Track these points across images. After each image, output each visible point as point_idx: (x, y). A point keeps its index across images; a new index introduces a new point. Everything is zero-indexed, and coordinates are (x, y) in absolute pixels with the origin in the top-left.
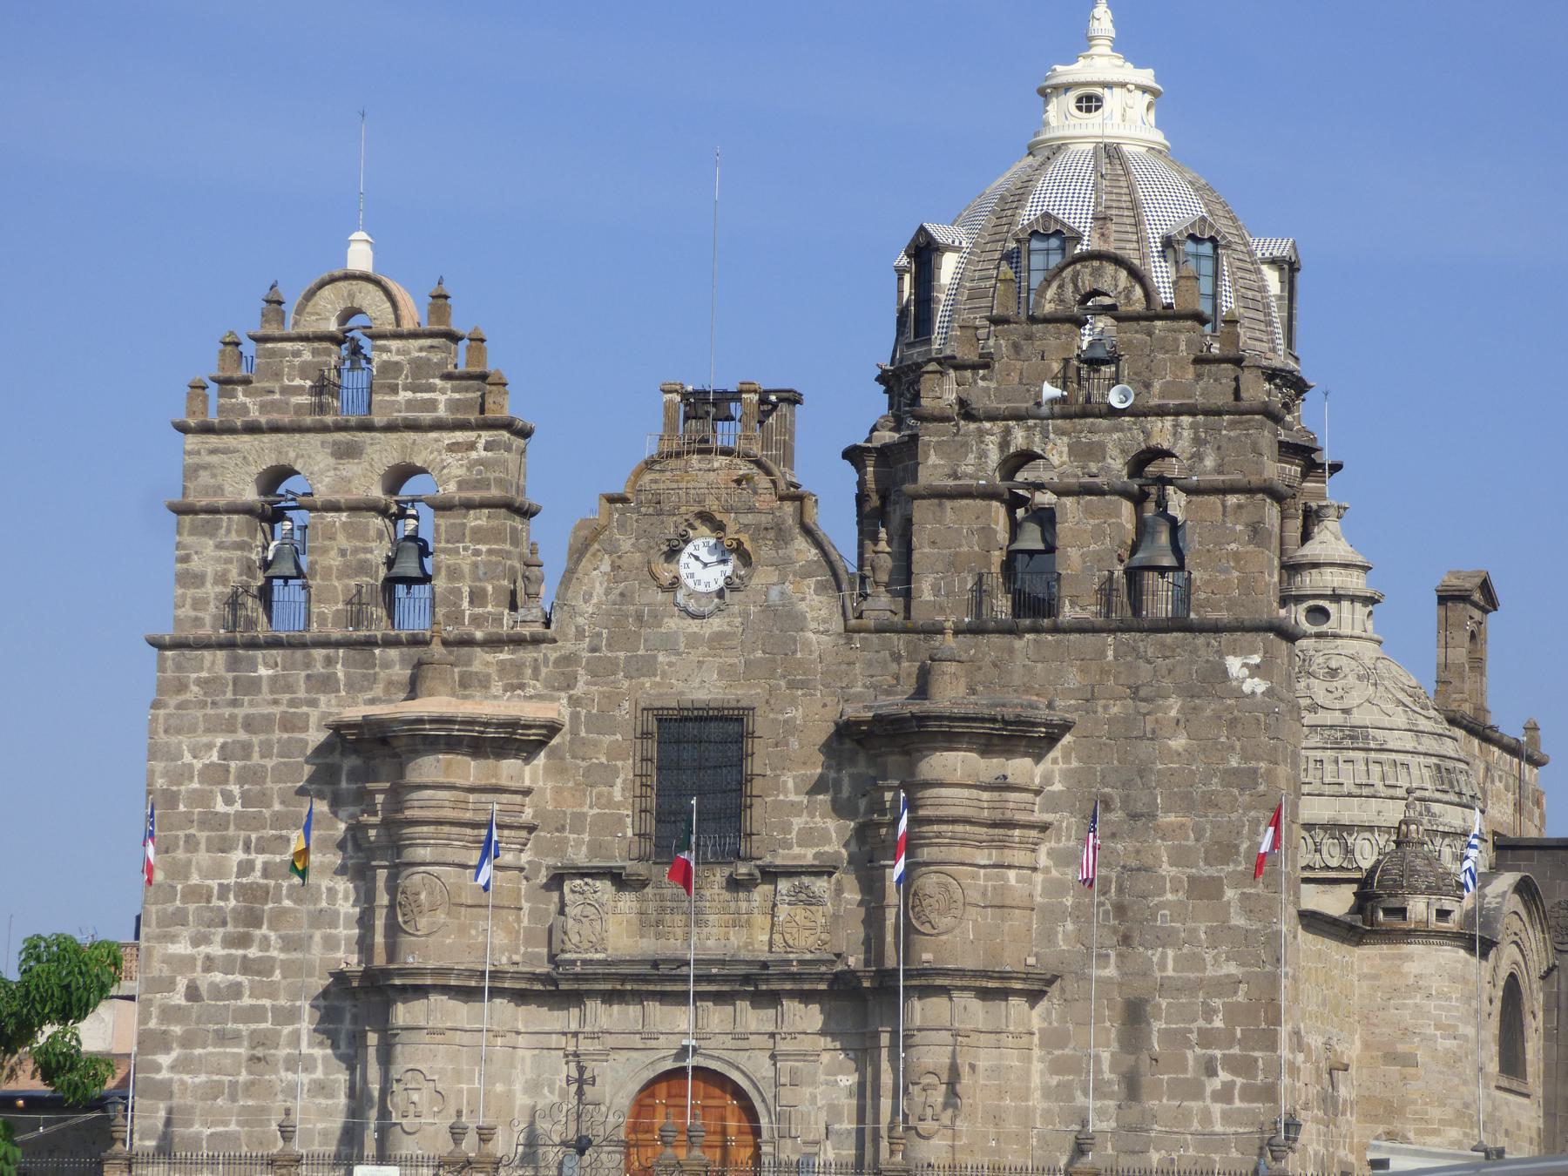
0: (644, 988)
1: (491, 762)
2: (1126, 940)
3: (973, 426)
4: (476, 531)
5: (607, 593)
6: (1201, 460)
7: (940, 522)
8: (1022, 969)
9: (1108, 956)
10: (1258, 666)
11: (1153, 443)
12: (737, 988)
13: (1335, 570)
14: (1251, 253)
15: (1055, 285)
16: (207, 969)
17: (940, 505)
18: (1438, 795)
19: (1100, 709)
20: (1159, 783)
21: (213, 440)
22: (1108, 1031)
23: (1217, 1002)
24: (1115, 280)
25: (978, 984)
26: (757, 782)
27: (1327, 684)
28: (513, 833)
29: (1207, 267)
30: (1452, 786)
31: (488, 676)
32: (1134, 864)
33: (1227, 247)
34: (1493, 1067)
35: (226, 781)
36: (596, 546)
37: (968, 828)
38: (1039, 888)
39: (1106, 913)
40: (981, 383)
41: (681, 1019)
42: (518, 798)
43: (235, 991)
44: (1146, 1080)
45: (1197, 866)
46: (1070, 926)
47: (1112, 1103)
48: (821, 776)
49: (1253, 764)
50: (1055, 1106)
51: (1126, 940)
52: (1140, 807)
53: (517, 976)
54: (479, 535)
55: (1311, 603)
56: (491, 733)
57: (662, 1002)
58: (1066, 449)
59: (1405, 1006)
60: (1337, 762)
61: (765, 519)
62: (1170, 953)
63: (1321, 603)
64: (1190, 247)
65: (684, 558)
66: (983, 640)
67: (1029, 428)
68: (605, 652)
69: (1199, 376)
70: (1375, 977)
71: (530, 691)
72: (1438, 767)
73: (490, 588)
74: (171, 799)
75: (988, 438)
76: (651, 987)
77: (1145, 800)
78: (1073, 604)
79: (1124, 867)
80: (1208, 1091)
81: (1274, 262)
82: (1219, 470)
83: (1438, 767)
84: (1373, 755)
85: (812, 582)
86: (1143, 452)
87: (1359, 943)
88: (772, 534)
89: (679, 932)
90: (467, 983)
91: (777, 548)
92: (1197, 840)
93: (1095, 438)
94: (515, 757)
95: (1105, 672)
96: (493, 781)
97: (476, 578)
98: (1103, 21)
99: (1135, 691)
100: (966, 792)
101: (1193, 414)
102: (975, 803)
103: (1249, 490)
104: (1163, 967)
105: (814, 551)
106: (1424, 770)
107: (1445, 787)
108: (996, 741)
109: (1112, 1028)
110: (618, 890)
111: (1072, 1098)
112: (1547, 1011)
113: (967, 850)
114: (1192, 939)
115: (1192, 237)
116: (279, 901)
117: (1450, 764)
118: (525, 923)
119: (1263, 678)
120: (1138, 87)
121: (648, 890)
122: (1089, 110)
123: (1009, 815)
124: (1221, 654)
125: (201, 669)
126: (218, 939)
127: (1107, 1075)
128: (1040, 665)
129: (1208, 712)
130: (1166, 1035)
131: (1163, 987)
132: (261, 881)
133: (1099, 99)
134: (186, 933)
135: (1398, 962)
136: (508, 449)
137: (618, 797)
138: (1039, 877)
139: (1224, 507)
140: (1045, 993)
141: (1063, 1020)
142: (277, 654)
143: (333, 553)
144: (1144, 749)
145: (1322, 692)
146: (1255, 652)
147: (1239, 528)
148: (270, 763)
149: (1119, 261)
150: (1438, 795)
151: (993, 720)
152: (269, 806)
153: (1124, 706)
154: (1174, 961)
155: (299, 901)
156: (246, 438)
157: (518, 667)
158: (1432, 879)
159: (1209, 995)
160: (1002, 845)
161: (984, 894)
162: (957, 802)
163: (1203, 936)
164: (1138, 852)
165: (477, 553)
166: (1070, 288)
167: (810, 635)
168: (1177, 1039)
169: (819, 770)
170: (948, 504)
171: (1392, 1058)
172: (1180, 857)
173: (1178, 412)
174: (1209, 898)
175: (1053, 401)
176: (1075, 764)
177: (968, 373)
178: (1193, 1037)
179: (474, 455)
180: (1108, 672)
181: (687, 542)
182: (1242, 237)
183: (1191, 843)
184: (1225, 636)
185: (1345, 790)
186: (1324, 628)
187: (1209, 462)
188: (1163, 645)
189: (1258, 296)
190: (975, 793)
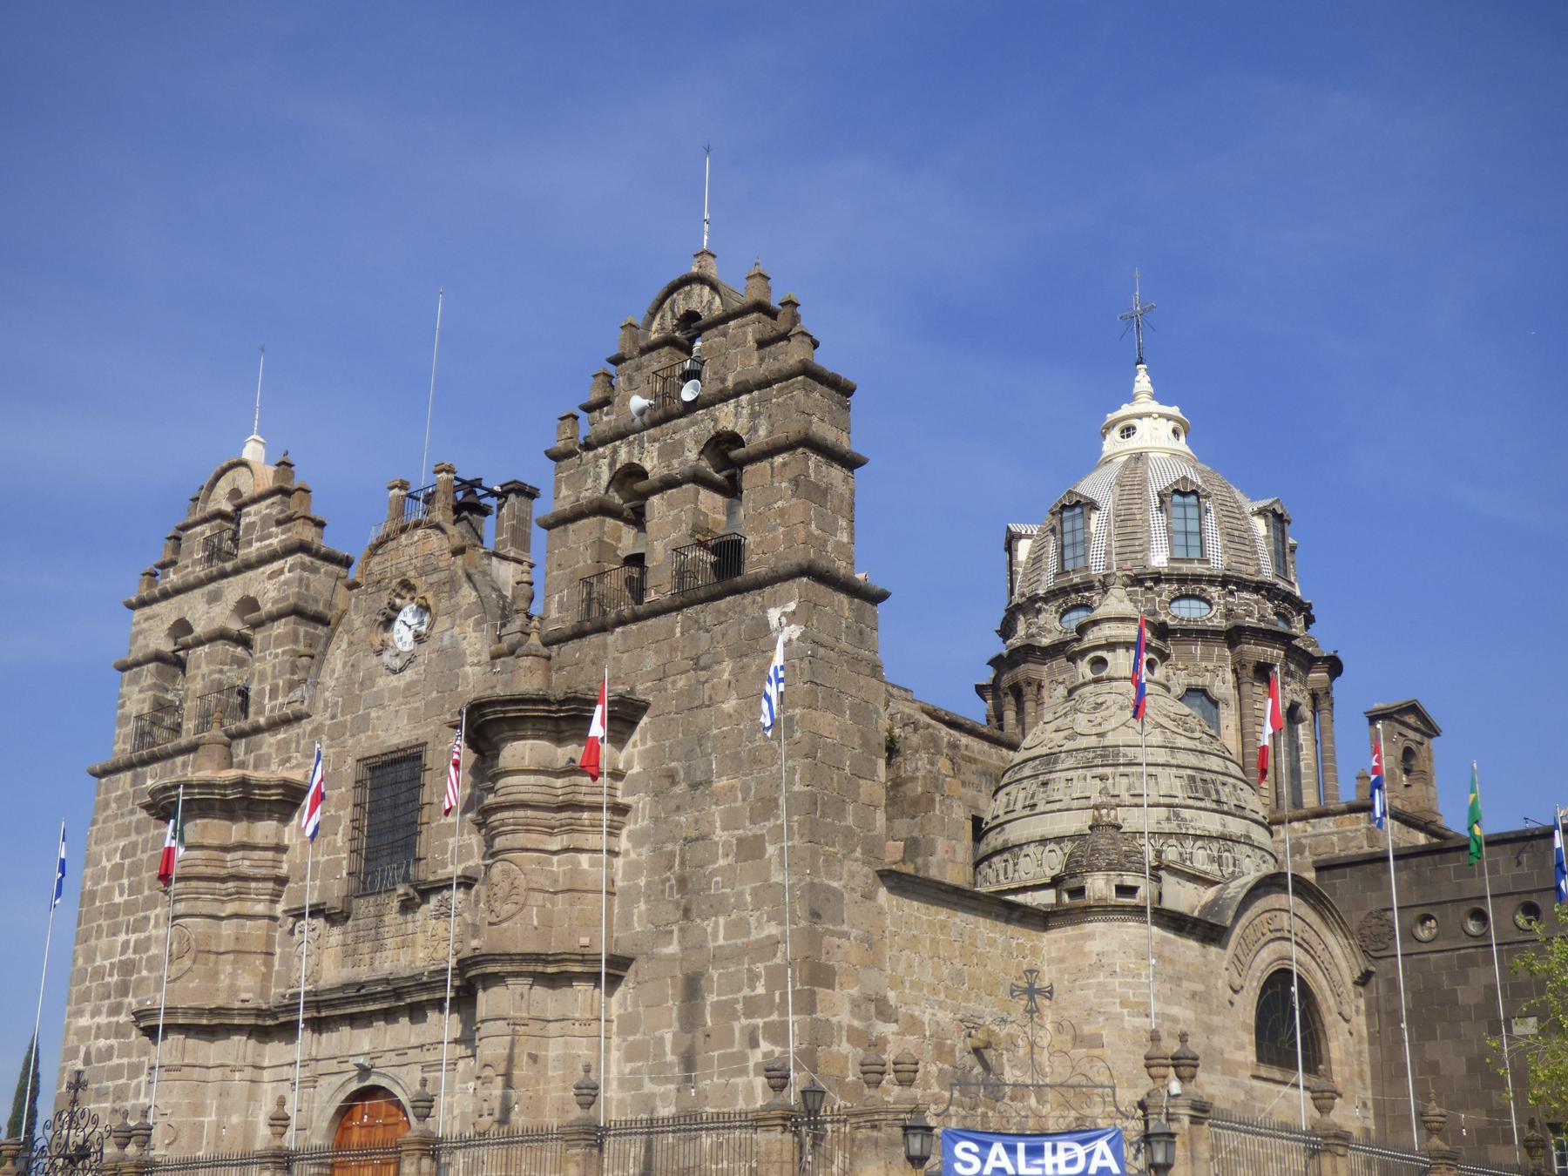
0: (338, 1012)
1: (244, 824)
2: (686, 913)
3: (591, 454)
4: (277, 638)
5: (344, 666)
6: (756, 431)
10: (794, 613)
11: (720, 427)
13: (1112, 625)
14: (1240, 508)
15: (658, 317)
16: (97, 1037)
20: (714, 748)
21: (147, 610)
22: (670, 1009)
23: (760, 967)
24: (700, 299)
25: (531, 969)
26: (426, 810)
27: (1091, 717)
28: (260, 885)
29: (1192, 512)
30: (1207, 793)
32: (694, 834)
33: (1207, 497)
34: (1249, 1054)
35: (121, 877)
37: (530, 813)
39: (671, 887)
40: (605, 418)
41: (361, 1042)
42: (270, 855)
43: (108, 1053)
44: (699, 1058)
45: (744, 828)
46: (643, 906)
47: (672, 1087)
48: (470, 795)
50: (628, 1095)
51: (686, 913)
53: (243, 1012)
54: (279, 641)
55: (1092, 655)
56: (232, 795)
57: (352, 1025)
58: (655, 454)
59: (1089, 986)
61: (443, 575)
62: (722, 920)
63: (1099, 653)
64: (1177, 499)
65: (398, 625)
66: (586, 641)
67: (630, 444)
68: (340, 718)
69: (762, 359)
70: (1061, 960)
71: (294, 762)
72: (1192, 779)
74: (93, 895)
75: (602, 461)
80: (751, 1064)
81: (1261, 513)
82: (770, 433)
83: (1192, 779)
84: (1122, 769)
85: (471, 621)
87: (1046, 928)
88: (447, 588)
89: (367, 957)
90: (196, 1021)
93: (676, 437)
94: (270, 818)
95: (673, 649)
97: (275, 677)
98: (1143, 382)
99: (696, 659)
100: (532, 779)
101: (750, 391)
102: (543, 789)
103: (789, 447)
104: (715, 937)
106: (1178, 782)
107: (1200, 795)
108: (564, 726)
109: (673, 1006)
111: (640, 1085)
112: (1369, 1015)
113: (534, 836)
114: (740, 905)
115: (1177, 492)
117: (1207, 776)
118: (276, 967)
119: (798, 624)
120: (1161, 416)
121: (350, 923)
123: (580, 797)
124: (764, 609)
127: (670, 1058)
130: (717, 1006)
131: (721, 957)
134: (89, 1007)
136: (314, 570)
137: (339, 843)
138: (619, 862)
141: (635, 1004)
142: (157, 766)
143: (199, 679)
144: (702, 716)
148: (145, 856)
149: (701, 280)
151: (545, 701)
152: (141, 892)
153: (689, 679)
155: (150, 970)
156: (164, 603)
157: (287, 742)
159: (753, 961)
161: (556, 881)
162: (522, 789)
163: (749, 898)
164: (697, 821)
165: (276, 656)
166: (669, 315)
167: (468, 669)
168: (726, 1011)
170: (571, 527)
171: (1078, 1040)
172: (731, 822)
173: (737, 394)
174: (754, 858)
175: (642, 412)
176: (649, 744)
177: (597, 413)
178: (739, 1007)
179: (282, 578)
180: (676, 649)
181: (398, 610)
183: (739, 804)
184: (768, 590)
186: (1104, 674)
187: (762, 432)
188: (719, 611)
190: (543, 779)
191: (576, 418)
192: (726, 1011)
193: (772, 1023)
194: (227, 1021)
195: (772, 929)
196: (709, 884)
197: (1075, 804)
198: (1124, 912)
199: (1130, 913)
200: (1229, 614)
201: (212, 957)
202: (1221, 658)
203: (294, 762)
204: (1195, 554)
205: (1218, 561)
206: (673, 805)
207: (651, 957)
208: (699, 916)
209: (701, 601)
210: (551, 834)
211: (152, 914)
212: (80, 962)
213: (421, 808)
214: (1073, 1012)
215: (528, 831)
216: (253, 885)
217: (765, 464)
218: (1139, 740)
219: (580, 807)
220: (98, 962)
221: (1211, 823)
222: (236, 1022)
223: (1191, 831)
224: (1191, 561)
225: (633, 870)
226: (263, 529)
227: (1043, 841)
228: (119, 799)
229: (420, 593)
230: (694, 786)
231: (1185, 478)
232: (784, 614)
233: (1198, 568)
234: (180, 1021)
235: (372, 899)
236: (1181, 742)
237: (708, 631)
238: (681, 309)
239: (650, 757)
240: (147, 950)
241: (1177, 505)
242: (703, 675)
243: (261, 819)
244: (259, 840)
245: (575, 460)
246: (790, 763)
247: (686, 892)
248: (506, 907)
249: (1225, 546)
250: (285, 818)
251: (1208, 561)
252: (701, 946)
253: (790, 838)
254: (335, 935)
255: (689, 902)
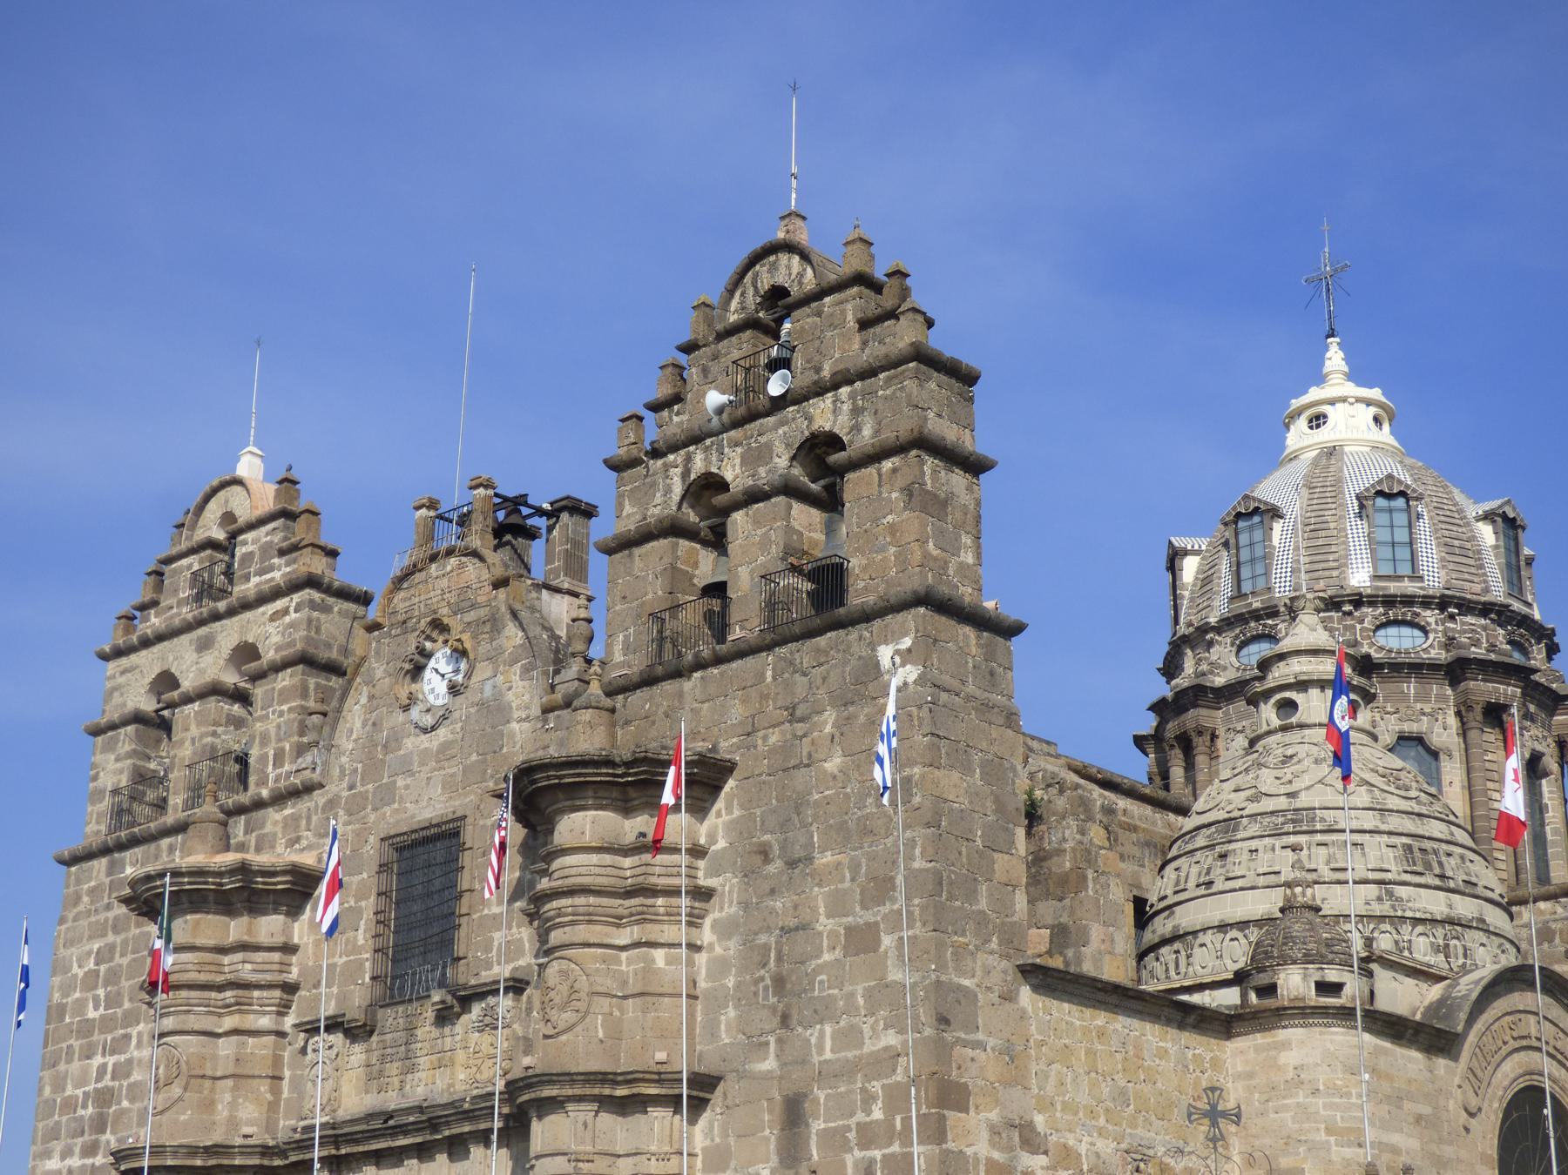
1: (245, 919)
2: (785, 1020)
3: (660, 462)
4: (281, 692)
5: (364, 725)
6: (860, 430)
7: (629, 574)
8: (655, 1068)
9: (767, 1044)
10: (909, 650)
11: (815, 427)
12: (429, 1138)
13: (1303, 659)
14: (1460, 511)
17: (630, 555)
18: (1407, 878)
19: (760, 742)
20: (816, 817)
21: (124, 662)
22: (767, 1139)
23: (876, 1086)
24: (788, 272)
25: (596, 1091)
27: (1279, 773)
28: (265, 994)
29: (1401, 519)
31: (275, 834)
33: (1417, 499)
35: (95, 987)
36: (358, 680)
37: (592, 900)
38: (703, 971)
39: (766, 989)
40: (676, 419)
42: (276, 956)
45: (854, 914)
48: (520, 880)
49: (907, 771)
51: (785, 1020)
52: (798, 852)
54: (284, 696)
55: (1278, 696)
56: (229, 884)
57: (378, 1165)
58: (738, 461)
59: (1286, 1108)
60: (1273, 849)
61: (483, 612)
62: (828, 1029)
63: (1287, 694)
64: (1381, 502)
65: (428, 674)
66: (656, 690)
67: (707, 449)
68: (360, 789)
69: (865, 343)
70: (1250, 1075)
71: (304, 843)
72: (1408, 848)
73: (288, 747)
74: (61, 1010)
75: (673, 471)
76: (361, 1149)
77: (802, 840)
78: (742, 628)
79: (782, 929)
81: (1488, 517)
82: (877, 432)
83: (1408, 848)
84: (1319, 837)
85: (517, 668)
86: (807, 440)
87: (1228, 1034)
88: (487, 628)
89: (396, 1081)
90: (189, 1162)
91: (492, 640)
92: (853, 880)
93: (763, 440)
94: (276, 911)
95: (764, 697)
96: (246, 938)
97: (280, 740)
98: (1335, 359)
99: (792, 709)
100: (594, 858)
101: (850, 382)
102: (609, 871)
103: (900, 449)
104: (821, 1050)
105: (521, 634)
106: (1391, 853)
107: (1419, 869)
108: (632, 793)
109: (770, 1135)
110: (353, 1042)
113: (598, 928)
114: (851, 1009)
115: (1380, 493)
116: (119, 1103)
117: (1427, 845)
118: (285, 1095)
119: (914, 663)
120: (1358, 400)
121: (374, 1038)
122: (1318, 426)
123: (654, 880)
125: (90, 879)
126: (77, 1150)
128: (706, 705)
129: (862, 719)
130: (824, 1134)
131: (828, 1074)
132: (110, 1084)
133: (1325, 416)
134: (58, 1146)
135: (1273, 1053)
136: (326, 609)
137: (361, 942)
138: (702, 959)
139: (880, 475)
140: (708, 1101)
142: (138, 851)
143: (187, 743)
145: (1270, 780)
146: (906, 635)
147: (894, 495)
148: (125, 961)
149: (789, 247)
150: (1407, 878)
151: (609, 763)
153: (783, 733)
154: (833, 1038)
155: (132, 1100)
156: (144, 653)
157: (295, 818)
158: (1311, 946)
159: (868, 1078)
160: (642, 918)
161: (625, 982)
162: (583, 870)
163: (861, 1001)
164: (796, 907)
165: (281, 714)
166: (751, 292)
167: (514, 726)
168: (836, 1141)
169: (517, 874)
170: (637, 551)
172: (837, 907)
173: (835, 386)
174: (866, 951)
175: (720, 411)
176: (737, 813)
177: (665, 413)
178: (852, 1135)
179: (287, 619)
181: (429, 656)
182: (1452, 499)
183: (847, 885)
184: (877, 623)
185: (1283, 879)
186: (1294, 720)
187: (867, 432)
188: (818, 650)
189: (1468, 545)
190: (607, 859)
191: (641, 419)
192: (836, 1141)
193: (893, 1155)
194: (226, 1162)
195: (891, 1039)
196: (812, 983)
197: (1262, 881)
198: (1327, 1015)
199: (1334, 1016)
200: (1449, 643)
201: (208, 1083)
202: (1442, 698)
203: (304, 843)
204: (1405, 569)
205: (1434, 578)
206: (766, 887)
207: (742, 1075)
208: (800, 1023)
209: (796, 639)
210: (618, 926)
211: (134, 1032)
212: (47, 1091)
213: (460, 896)
214: (1267, 1141)
215: (590, 922)
216: (256, 993)
217: (871, 471)
218: (1340, 801)
219: (653, 892)
220: (69, 1091)
221: (1435, 903)
222: (237, 1162)
223: (1409, 914)
224: (1399, 578)
225: (719, 967)
226: (262, 562)
227: (1223, 927)
228: (92, 892)
229: (455, 634)
230: (792, 864)
231: (1390, 477)
232: (897, 652)
233: (1409, 587)
234: (169, 1163)
235: (401, 1009)
236: (1394, 802)
237: (805, 675)
238: (765, 284)
239: (739, 830)
240: (128, 1075)
241: (1381, 510)
242: (800, 728)
243: (265, 913)
244: (263, 938)
245: (640, 470)
246: (908, 834)
247: (784, 995)
248: (564, 1016)
249: (1442, 560)
250: (294, 912)
251: (1421, 578)
252: (804, 1062)
253: (910, 927)
254: (357, 1054)
255: (788, 1006)
